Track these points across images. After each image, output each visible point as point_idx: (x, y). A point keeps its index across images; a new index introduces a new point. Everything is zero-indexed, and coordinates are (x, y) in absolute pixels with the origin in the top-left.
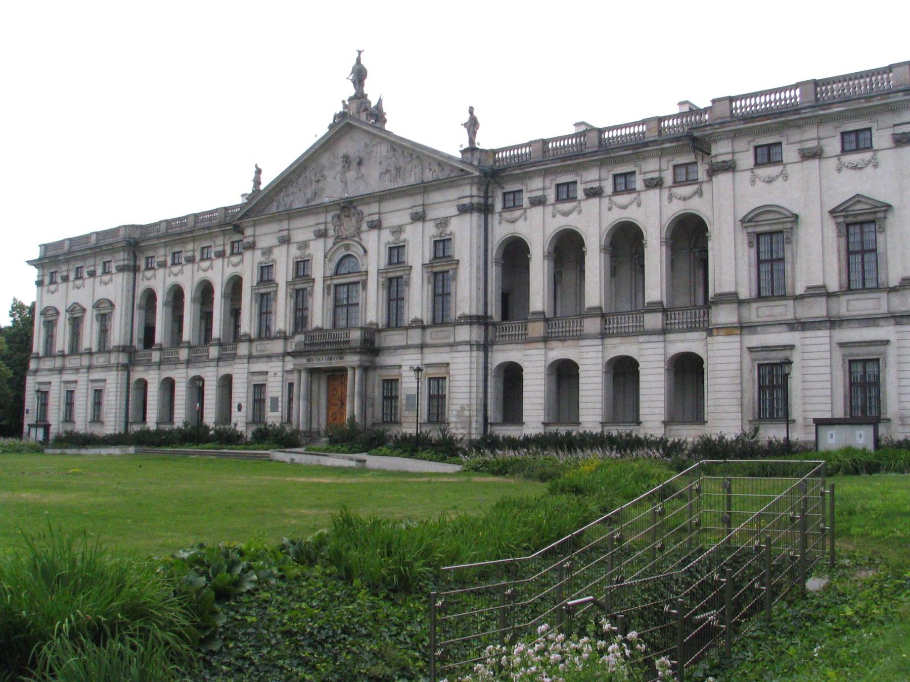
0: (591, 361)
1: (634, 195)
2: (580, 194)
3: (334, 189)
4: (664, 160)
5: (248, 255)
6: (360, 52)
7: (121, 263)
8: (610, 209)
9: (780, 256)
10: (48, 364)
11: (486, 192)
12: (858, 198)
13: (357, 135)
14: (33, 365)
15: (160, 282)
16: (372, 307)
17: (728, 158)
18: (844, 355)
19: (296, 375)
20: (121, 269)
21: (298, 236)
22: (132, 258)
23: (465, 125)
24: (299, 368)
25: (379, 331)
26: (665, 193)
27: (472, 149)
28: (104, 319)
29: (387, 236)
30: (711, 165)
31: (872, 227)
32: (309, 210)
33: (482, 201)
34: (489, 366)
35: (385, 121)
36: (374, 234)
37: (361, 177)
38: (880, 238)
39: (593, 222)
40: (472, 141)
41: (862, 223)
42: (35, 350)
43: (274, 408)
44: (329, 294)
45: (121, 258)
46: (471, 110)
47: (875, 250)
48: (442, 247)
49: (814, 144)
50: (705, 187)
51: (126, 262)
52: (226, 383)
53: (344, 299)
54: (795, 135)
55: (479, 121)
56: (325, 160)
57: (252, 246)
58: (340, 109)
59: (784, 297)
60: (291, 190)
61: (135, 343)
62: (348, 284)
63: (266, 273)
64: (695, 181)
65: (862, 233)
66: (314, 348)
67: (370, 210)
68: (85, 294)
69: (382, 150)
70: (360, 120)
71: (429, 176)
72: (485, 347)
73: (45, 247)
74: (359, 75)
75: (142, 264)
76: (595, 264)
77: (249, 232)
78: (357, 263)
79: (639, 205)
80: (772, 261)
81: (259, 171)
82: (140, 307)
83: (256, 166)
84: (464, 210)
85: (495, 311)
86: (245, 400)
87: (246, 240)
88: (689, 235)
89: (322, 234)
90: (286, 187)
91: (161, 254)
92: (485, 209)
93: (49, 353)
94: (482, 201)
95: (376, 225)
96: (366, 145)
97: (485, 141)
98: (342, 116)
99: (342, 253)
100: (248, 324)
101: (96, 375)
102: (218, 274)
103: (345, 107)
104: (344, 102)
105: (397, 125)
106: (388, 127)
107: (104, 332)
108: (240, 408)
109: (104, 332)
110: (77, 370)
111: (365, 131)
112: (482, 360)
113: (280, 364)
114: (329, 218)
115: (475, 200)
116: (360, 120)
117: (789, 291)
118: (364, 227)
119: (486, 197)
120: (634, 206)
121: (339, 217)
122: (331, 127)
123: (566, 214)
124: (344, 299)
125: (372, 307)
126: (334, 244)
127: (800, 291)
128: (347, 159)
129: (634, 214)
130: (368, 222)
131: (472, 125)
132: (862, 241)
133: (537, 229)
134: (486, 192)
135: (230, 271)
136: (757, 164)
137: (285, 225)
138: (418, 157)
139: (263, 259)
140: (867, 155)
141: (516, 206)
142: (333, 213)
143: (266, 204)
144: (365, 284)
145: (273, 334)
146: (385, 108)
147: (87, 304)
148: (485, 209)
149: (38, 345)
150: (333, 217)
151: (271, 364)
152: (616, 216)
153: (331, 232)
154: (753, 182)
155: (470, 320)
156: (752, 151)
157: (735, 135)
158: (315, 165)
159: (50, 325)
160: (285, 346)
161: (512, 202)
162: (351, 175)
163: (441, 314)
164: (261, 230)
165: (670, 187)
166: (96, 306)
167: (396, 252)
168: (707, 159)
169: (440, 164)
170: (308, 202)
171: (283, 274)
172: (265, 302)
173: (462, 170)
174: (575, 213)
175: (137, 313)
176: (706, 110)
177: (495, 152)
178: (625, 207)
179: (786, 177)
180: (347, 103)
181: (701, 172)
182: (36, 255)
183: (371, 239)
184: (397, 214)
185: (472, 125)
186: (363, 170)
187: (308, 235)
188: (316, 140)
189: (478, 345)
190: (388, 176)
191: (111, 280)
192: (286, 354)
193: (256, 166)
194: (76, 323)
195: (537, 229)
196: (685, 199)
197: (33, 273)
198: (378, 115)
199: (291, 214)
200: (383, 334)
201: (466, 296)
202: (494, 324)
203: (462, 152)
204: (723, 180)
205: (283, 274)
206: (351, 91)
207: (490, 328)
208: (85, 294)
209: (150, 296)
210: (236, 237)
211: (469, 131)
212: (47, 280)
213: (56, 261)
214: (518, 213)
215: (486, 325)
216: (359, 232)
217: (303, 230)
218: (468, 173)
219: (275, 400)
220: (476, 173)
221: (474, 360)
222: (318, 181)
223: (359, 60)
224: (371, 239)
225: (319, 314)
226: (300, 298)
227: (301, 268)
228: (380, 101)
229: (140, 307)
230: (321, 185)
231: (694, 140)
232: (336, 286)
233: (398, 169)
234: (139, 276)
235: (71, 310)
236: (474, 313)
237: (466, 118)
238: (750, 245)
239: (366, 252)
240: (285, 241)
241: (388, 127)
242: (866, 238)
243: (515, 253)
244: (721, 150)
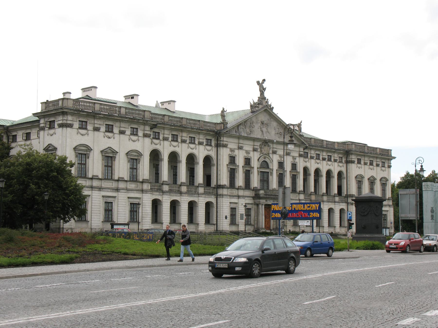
16: (274, 184)
36: (274, 155)
43: (242, 219)
53: (265, 178)
57: (225, 146)
66: (272, 197)
76: (323, 180)
84: (300, 156)
86: (229, 214)
89: (255, 150)
95: (274, 152)
102: (201, 152)
108: (226, 217)
110: (117, 190)
118: (271, 152)
124: (265, 178)
128: (262, 123)
139: (230, 153)
144: (272, 174)
151: (240, 200)
181: (344, 160)
205: (240, 162)
214: (307, 160)
217: (248, 146)
219: (242, 215)
225: (255, 182)
227: (248, 161)
230: (254, 129)
240: (240, 148)
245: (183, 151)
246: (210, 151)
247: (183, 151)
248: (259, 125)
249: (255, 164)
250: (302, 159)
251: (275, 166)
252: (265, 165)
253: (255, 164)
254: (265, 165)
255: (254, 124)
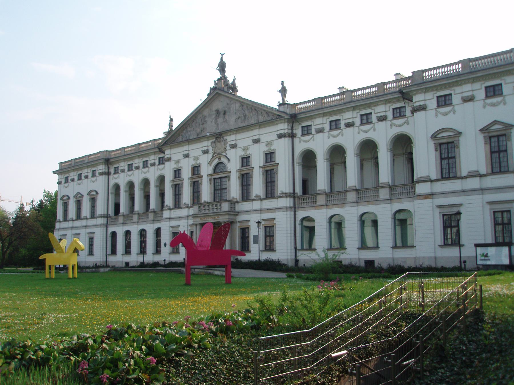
0: (350, 215)
1: (372, 125)
2: (342, 126)
3: (211, 128)
4: (388, 106)
5: (167, 164)
6: (222, 55)
7: (101, 171)
8: (359, 133)
9: (453, 155)
10: (65, 225)
11: (292, 127)
12: (495, 122)
13: (222, 98)
14: (57, 225)
15: (122, 179)
16: (234, 189)
17: (422, 103)
18: (491, 209)
19: (194, 227)
20: (101, 174)
21: (193, 154)
22: (107, 168)
23: (280, 91)
24: (196, 223)
25: (238, 202)
26: (389, 123)
27: (283, 104)
28: (93, 200)
29: (240, 153)
30: (413, 108)
31: (504, 138)
32: (199, 139)
33: (290, 131)
34: (297, 219)
35: (237, 91)
37: (225, 121)
38: (509, 143)
39: (350, 140)
40: (283, 100)
41: (498, 136)
42: (58, 218)
44: (210, 183)
45: (101, 168)
46: (283, 83)
47: (506, 151)
48: (269, 156)
49: (469, 94)
50: (410, 119)
51: (104, 171)
52: (158, 232)
54: (458, 89)
55: (287, 89)
56: (206, 112)
57: (169, 159)
58: (213, 85)
59: (455, 178)
60: (189, 129)
61: (110, 213)
62: (221, 178)
63: (177, 173)
64: (404, 116)
65: (498, 141)
67: (231, 139)
68: (84, 187)
69: (237, 106)
70: (223, 90)
71: (261, 119)
72: (294, 209)
73: (61, 164)
74: (222, 67)
75: (112, 171)
77: (167, 152)
78: (225, 167)
79: (374, 130)
80: (448, 158)
81: (171, 120)
82: (112, 193)
83: (170, 117)
84: (280, 136)
85: (299, 190)
87: (166, 157)
88: (403, 145)
89: (206, 152)
90: (186, 128)
91: (123, 165)
92: (292, 136)
93: (65, 219)
94: (290, 131)
95: (234, 146)
96: (228, 104)
97: (291, 99)
98: (213, 89)
99: (216, 161)
100: (169, 200)
101: (89, 230)
103: (216, 84)
104: (215, 81)
105: (243, 92)
106: (239, 94)
107: (93, 207)
108: (165, 245)
109: (93, 207)
111: (227, 97)
112: (293, 216)
113: (186, 221)
114: (210, 144)
115: (286, 131)
116: (223, 90)
117: (458, 175)
118: (228, 147)
119: (292, 129)
120: (372, 130)
121: (214, 142)
122: (208, 95)
123: (335, 136)
125: (234, 189)
126: (213, 157)
127: (464, 174)
128: (218, 112)
129: (371, 135)
130: (230, 145)
131: (283, 91)
132: (499, 146)
133: (320, 144)
134: (292, 127)
135: (159, 173)
136: (439, 106)
137: (186, 148)
138: (255, 110)
139: (175, 166)
140: (499, 99)
141: (309, 133)
142: (211, 141)
143: (175, 137)
144: (229, 177)
145: (182, 206)
146: (237, 84)
147: (85, 194)
148: (292, 136)
149: (60, 215)
150: (212, 143)
152: (363, 136)
153: (211, 151)
154: (436, 116)
155: (285, 195)
156: (435, 99)
157: (426, 90)
158: (201, 116)
159: (66, 205)
160: (189, 212)
161: (307, 131)
162: (220, 120)
163: (270, 191)
164: (174, 151)
165: (391, 120)
166: (89, 194)
167: (245, 160)
168: (411, 104)
169: (267, 113)
170: (198, 135)
171: (186, 174)
172: (177, 189)
173: (279, 115)
174: (340, 135)
175: (110, 196)
176: (409, 78)
177: (295, 105)
178: (366, 132)
179: (454, 112)
180: (217, 82)
182: (57, 168)
183: (231, 153)
184: (244, 140)
185: (283, 91)
186: (226, 117)
187: (199, 152)
188: (201, 102)
189: (291, 208)
190: (240, 120)
191: (96, 180)
192: (188, 217)
193: (170, 117)
194: (79, 203)
195: (320, 144)
196: (399, 126)
197: (56, 177)
198: (233, 88)
199: (189, 141)
200: (240, 204)
201: (284, 182)
202: (298, 197)
203: (278, 105)
204: (419, 115)
206: (218, 75)
207: (296, 199)
208: (84, 187)
209: (117, 187)
210: (161, 155)
211: (282, 95)
212: (63, 181)
213: (68, 170)
215: (294, 197)
216: (225, 149)
217: (195, 150)
218: (282, 117)
220: (286, 117)
221: (289, 216)
222: (203, 124)
223: (222, 59)
224: (231, 153)
225: (206, 195)
226: (196, 186)
227: (196, 170)
228: (234, 81)
229: (112, 193)
230: (205, 126)
231: (404, 94)
232: (214, 179)
233: (245, 116)
234: (111, 177)
235: (75, 197)
236: (287, 191)
237: (280, 88)
238: (436, 150)
239: (229, 160)
241: (239, 94)
242: (501, 143)
243: (309, 159)
244: (418, 99)
245: (137, 177)
246: (162, 169)
247: (137, 177)
248: (214, 116)
249: (206, 171)
250: (287, 141)
251: (233, 166)
252: (219, 167)
253: (206, 171)
254: (219, 167)
255: (206, 119)
